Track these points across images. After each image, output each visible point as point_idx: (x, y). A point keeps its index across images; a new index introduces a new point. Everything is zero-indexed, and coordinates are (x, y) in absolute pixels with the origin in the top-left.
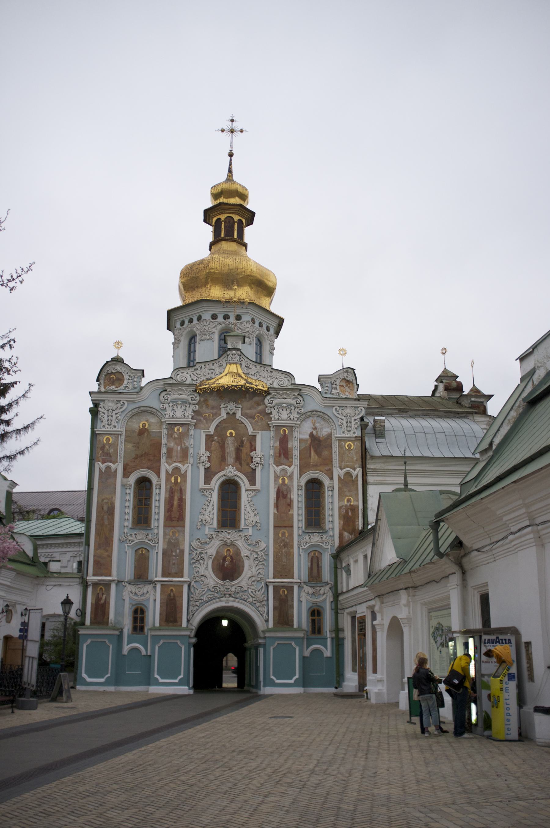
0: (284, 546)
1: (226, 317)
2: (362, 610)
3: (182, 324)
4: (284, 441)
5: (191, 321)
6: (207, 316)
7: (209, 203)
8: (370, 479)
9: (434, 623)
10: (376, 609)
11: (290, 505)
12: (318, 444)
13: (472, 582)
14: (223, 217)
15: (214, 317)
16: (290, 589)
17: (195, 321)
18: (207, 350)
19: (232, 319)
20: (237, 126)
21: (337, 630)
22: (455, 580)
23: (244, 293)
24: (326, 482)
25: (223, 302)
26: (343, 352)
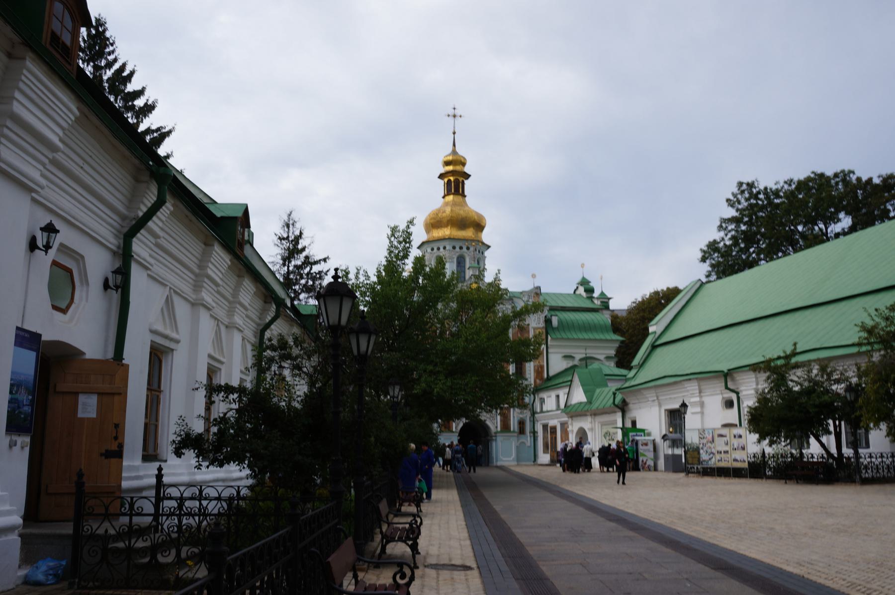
1: (461, 248)
2: (552, 423)
3: (432, 249)
5: (438, 249)
7: (443, 170)
8: (550, 351)
9: (605, 431)
10: (570, 422)
13: (630, 415)
15: (454, 248)
17: (442, 249)
19: (465, 249)
20: (458, 112)
21: (534, 433)
22: (620, 414)
23: (469, 233)
26: (534, 276)
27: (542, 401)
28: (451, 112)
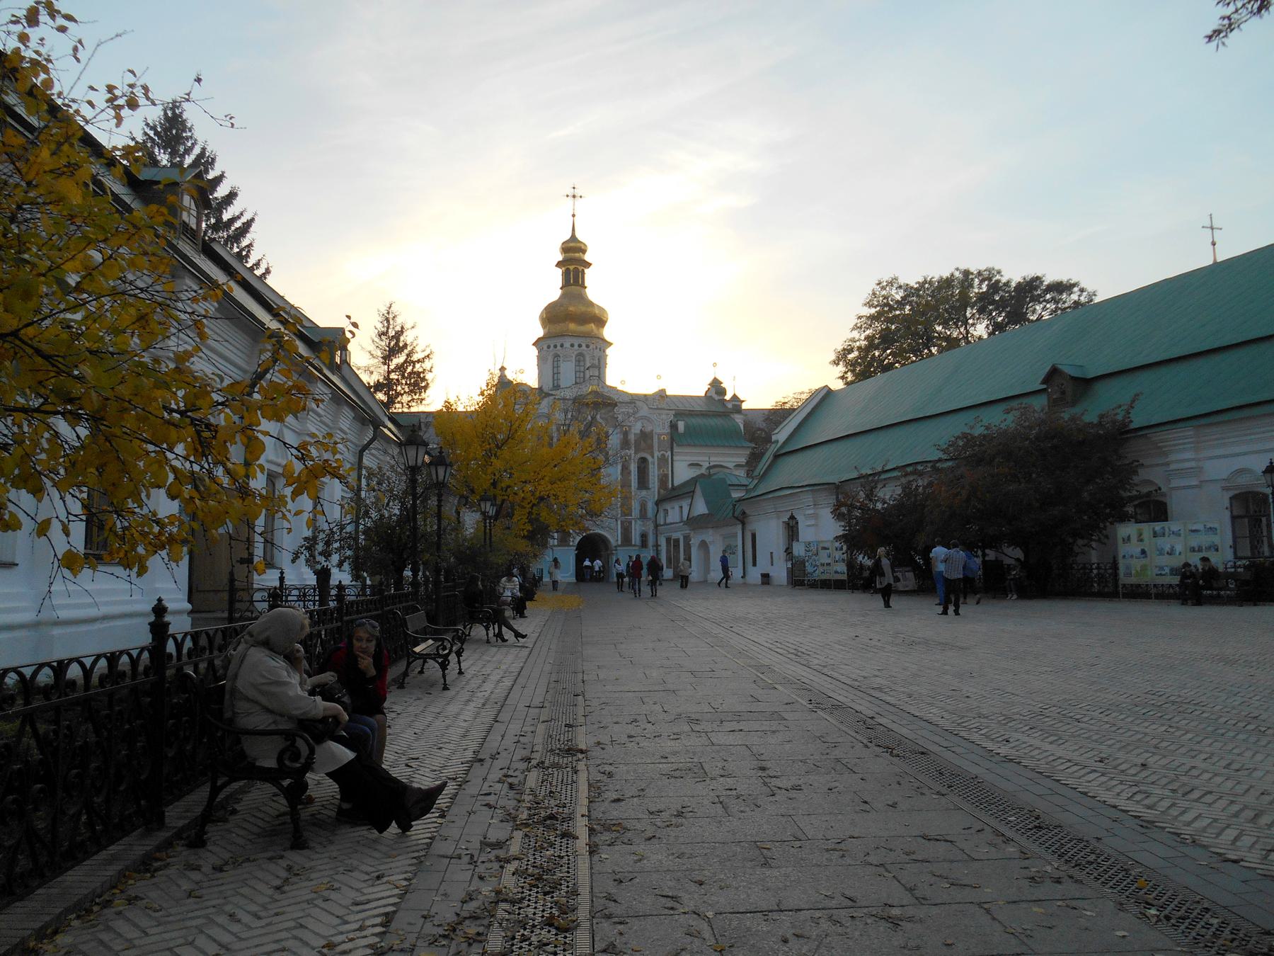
0: (626, 499)
1: (580, 346)
2: (675, 536)
4: (626, 434)
6: (567, 345)
7: (560, 258)
11: (630, 473)
12: (645, 436)
14: (571, 268)
15: (572, 345)
16: (630, 523)
18: (568, 372)
20: (578, 193)
21: (657, 546)
22: (740, 526)
24: (650, 459)
25: (572, 326)
26: (659, 377)
27: (666, 511)
28: (571, 192)
